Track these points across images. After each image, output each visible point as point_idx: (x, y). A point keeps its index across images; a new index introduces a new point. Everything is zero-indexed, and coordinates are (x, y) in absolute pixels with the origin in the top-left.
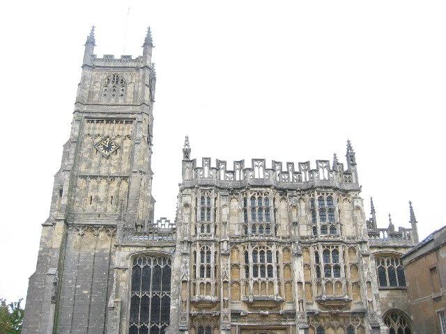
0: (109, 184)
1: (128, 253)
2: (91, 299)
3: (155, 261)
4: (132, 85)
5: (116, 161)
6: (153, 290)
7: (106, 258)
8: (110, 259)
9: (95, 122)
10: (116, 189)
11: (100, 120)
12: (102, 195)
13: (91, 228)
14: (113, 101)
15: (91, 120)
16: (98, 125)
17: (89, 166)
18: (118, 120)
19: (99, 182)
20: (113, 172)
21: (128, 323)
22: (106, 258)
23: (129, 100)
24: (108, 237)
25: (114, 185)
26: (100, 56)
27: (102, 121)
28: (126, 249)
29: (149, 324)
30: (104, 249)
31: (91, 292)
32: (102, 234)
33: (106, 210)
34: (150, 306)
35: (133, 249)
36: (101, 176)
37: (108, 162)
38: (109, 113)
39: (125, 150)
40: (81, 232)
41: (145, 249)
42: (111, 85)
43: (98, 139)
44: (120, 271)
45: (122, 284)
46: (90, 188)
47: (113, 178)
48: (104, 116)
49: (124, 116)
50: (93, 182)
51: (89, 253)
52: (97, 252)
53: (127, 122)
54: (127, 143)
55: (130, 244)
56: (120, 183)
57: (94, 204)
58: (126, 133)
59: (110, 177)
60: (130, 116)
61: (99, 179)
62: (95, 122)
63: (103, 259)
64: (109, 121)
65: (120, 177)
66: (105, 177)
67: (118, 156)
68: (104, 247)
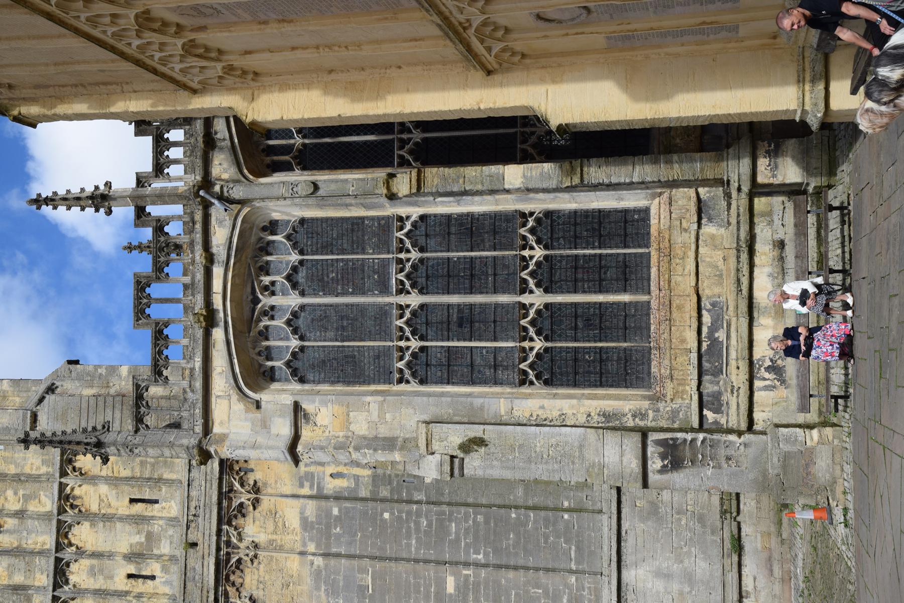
0: (85, 515)
1: (238, 407)
2: (477, 565)
3: (270, 290)
5: (10, 493)
6: (384, 289)
7: (335, 511)
8: (338, 497)
10: (104, 489)
19: (81, 552)
20: (47, 503)
21: (525, 390)
22: (335, 511)
24: (266, 503)
28: (219, 410)
29: (526, 299)
31: (451, 563)
33: (174, 522)
34: (454, 299)
35: (220, 383)
36: (59, 547)
41: (218, 334)
44: (306, 433)
45: (361, 426)
46: (99, 583)
47: (65, 498)
51: (317, 575)
52: (311, 548)
55: (199, 396)
57: (154, 568)
59: (61, 511)
61: (68, 554)
63: (338, 519)
65: (63, 474)
66: (62, 531)
68: (293, 520)
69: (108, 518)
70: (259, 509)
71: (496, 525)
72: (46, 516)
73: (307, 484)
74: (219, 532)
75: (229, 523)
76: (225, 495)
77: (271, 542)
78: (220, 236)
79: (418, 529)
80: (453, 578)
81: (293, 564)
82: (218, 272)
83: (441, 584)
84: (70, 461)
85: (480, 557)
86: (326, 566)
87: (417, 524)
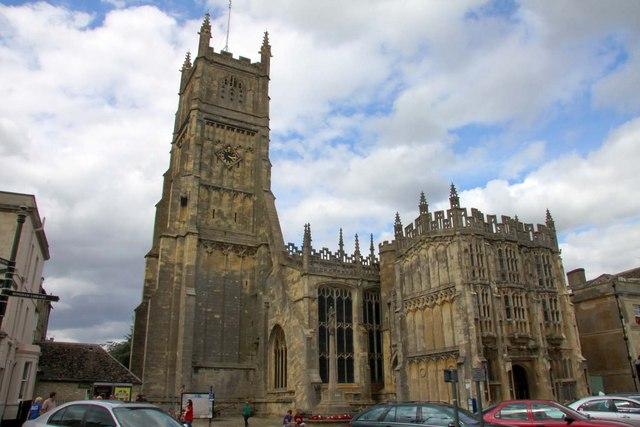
4: (251, 93)
9: (215, 125)
10: (240, 205)
11: (221, 125)
12: (225, 210)
13: (221, 246)
14: (231, 106)
15: (211, 122)
16: (218, 130)
17: (210, 175)
18: (241, 130)
23: (250, 110)
24: (238, 259)
25: (238, 201)
26: (217, 51)
27: (233, 130)
28: (314, 278)
30: (234, 271)
32: (231, 254)
35: (320, 278)
37: (231, 174)
38: (230, 119)
39: (247, 164)
40: (209, 249)
42: (229, 87)
43: (218, 147)
47: (237, 193)
48: (224, 120)
49: (246, 126)
50: (215, 194)
53: (248, 134)
54: (249, 156)
56: (243, 201)
58: (247, 146)
60: (253, 128)
62: (215, 125)
64: (231, 128)
66: (228, 191)
67: (240, 169)
69: (232, 205)
72: (231, 185)
76: (242, 247)
77: (227, 260)
78: (351, 282)
81: (222, 267)
82: (343, 281)
83: (218, 313)
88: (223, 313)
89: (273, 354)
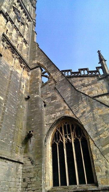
2: (4, 108)
70: (20, 66)
71: (12, 119)
73: (23, 79)
74: (19, 55)
75: (19, 58)
79: (13, 97)
80: (3, 99)
84: (24, 42)
85: (6, 111)
86: (9, 70)
87: (14, 98)
88: (7, 97)
89: (49, 148)
